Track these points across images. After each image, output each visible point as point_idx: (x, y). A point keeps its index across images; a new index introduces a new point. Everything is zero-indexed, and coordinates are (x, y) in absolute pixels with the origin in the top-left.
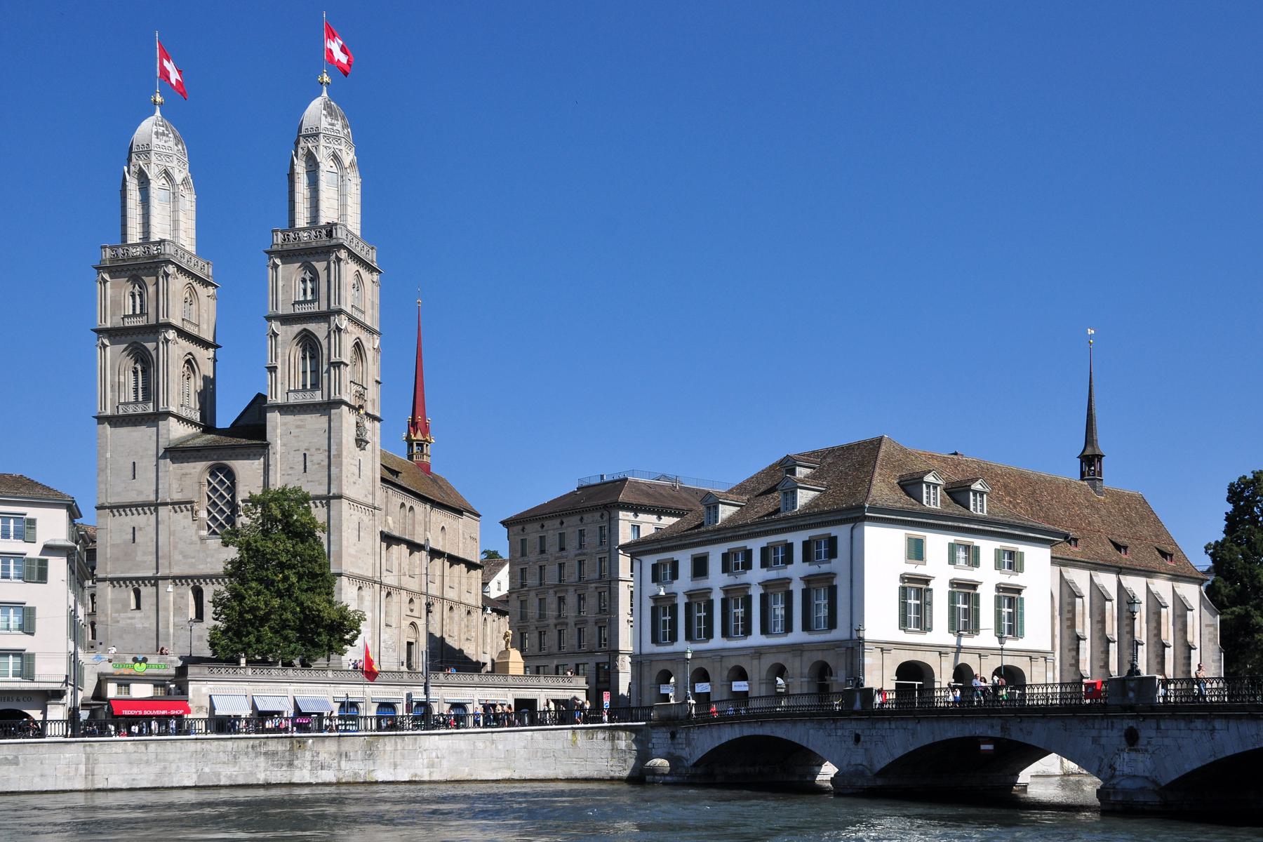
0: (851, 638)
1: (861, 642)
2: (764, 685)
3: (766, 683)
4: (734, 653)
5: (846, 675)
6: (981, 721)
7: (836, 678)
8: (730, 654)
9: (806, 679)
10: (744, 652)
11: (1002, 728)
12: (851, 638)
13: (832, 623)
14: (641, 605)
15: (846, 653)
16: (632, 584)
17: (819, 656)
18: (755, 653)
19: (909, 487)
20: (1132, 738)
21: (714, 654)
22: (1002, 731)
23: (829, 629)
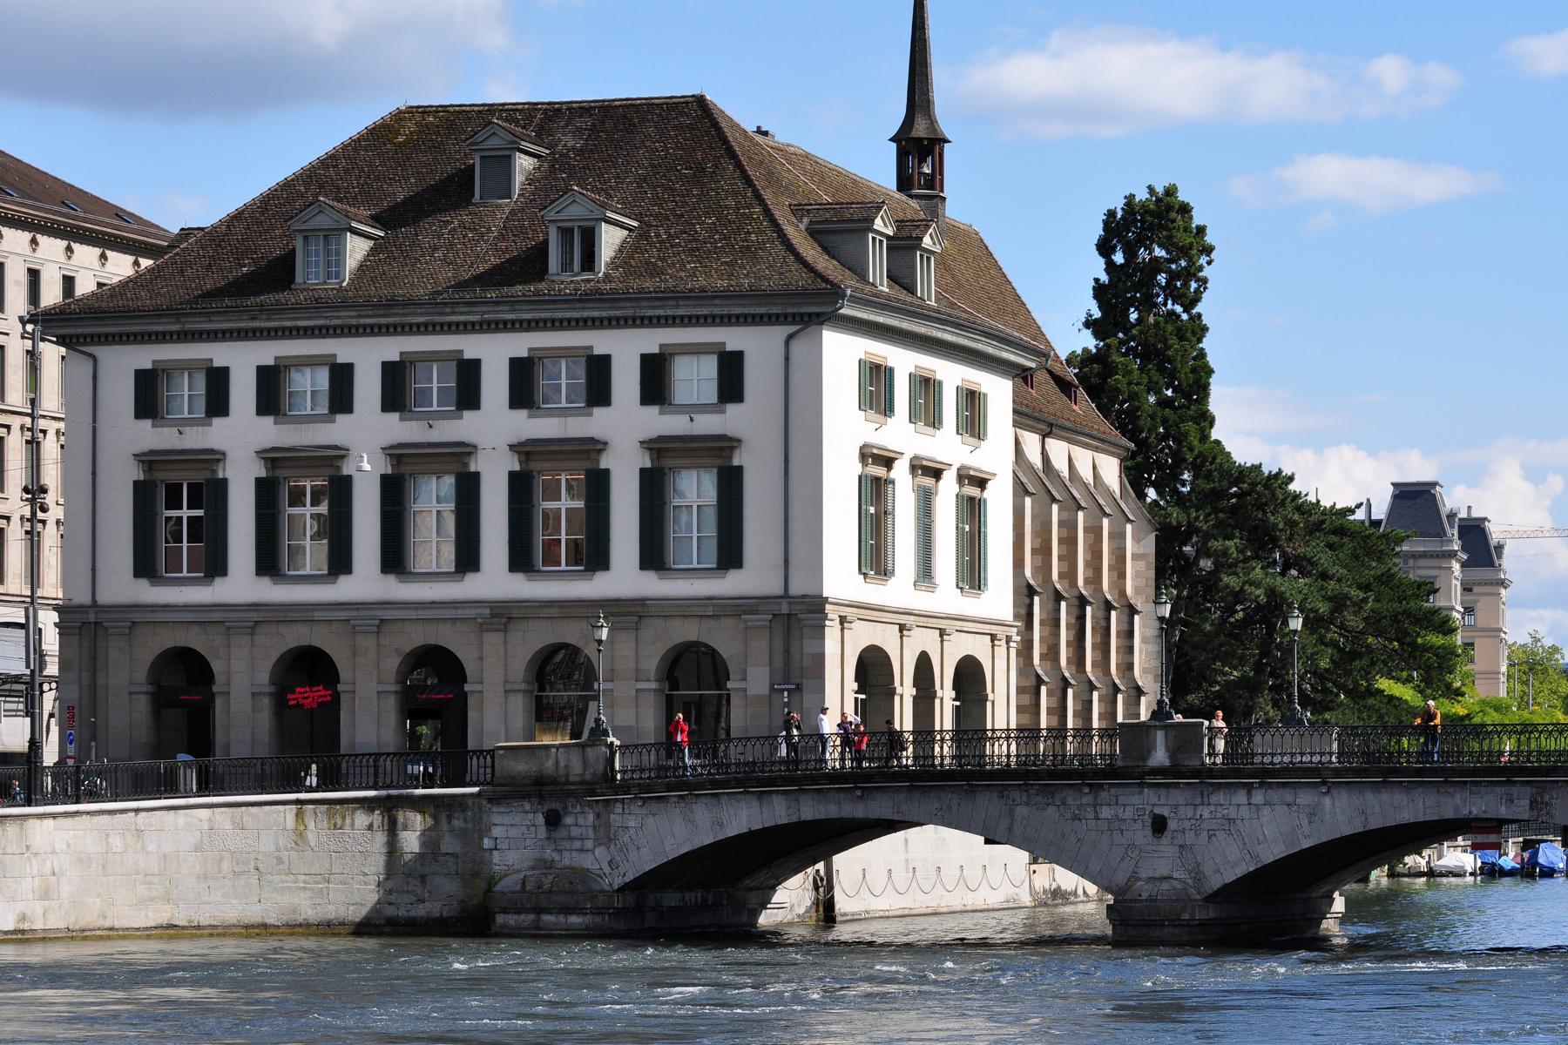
0: (786, 596)
1: (816, 606)
2: (653, 694)
3: (524, 691)
4: (422, 614)
5: (771, 676)
6: (1483, 790)
7: (742, 685)
8: (412, 614)
9: (654, 685)
10: (460, 613)
11: (1531, 802)
12: (786, 596)
13: (730, 555)
14: (94, 474)
15: (770, 628)
16: (61, 425)
17: (689, 632)
18: (493, 616)
19: (831, 238)
21: (355, 613)
22: (1531, 808)
23: (719, 568)
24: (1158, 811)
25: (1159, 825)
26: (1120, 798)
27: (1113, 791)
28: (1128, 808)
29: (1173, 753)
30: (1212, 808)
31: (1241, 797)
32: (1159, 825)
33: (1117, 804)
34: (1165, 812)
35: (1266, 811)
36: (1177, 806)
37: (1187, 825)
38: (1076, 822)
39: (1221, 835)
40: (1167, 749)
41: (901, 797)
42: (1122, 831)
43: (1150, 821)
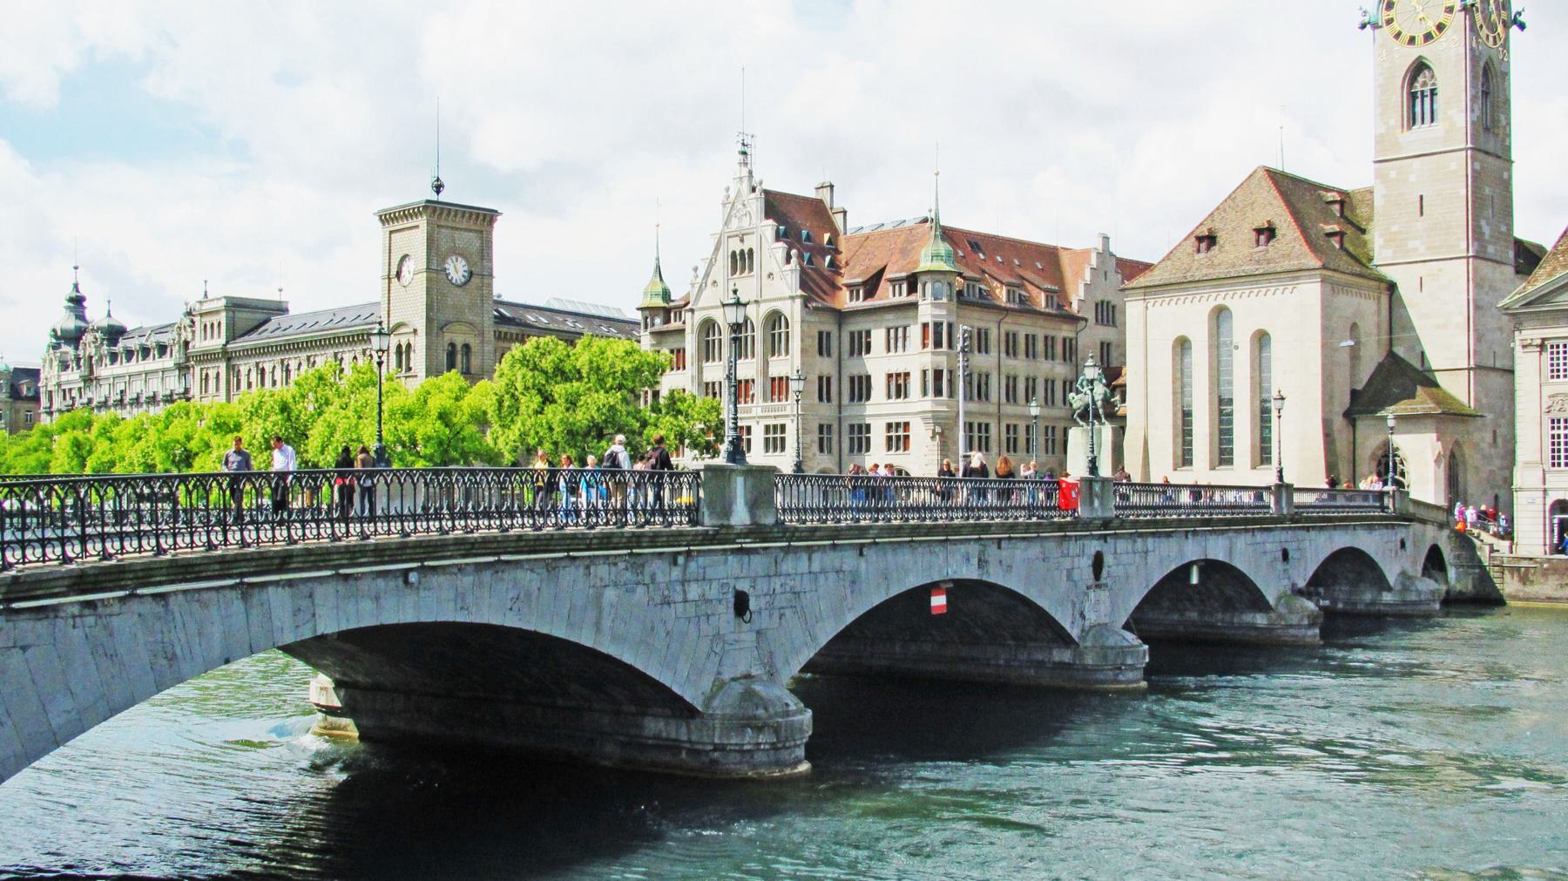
11: (980, 560)
20: (1098, 563)
24: (739, 588)
25: (741, 604)
26: (707, 569)
27: (701, 560)
28: (715, 584)
29: (753, 506)
30: (782, 579)
31: (803, 565)
32: (741, 604)
33: (704, 579)
34: (744, 586)
35: (822, 578)
36: (754, 579)
37: (763, 601)
38: (666, 606)
39: (788, 612)
40: (746, 504)
41: (467, 580)
42: (708, 616)
43: (733, 600)
